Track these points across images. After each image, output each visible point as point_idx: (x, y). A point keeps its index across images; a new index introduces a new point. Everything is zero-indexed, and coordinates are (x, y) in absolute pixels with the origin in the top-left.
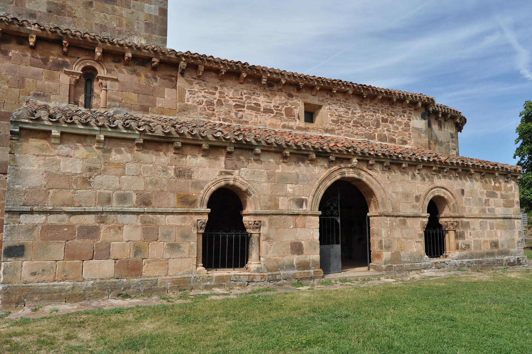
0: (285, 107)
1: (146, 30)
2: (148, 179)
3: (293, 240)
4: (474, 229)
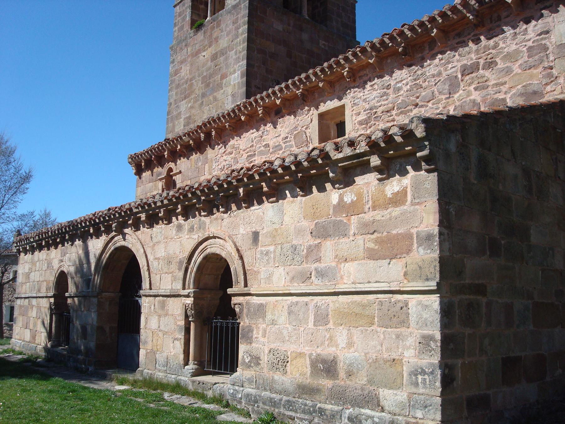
4: (273, 322)
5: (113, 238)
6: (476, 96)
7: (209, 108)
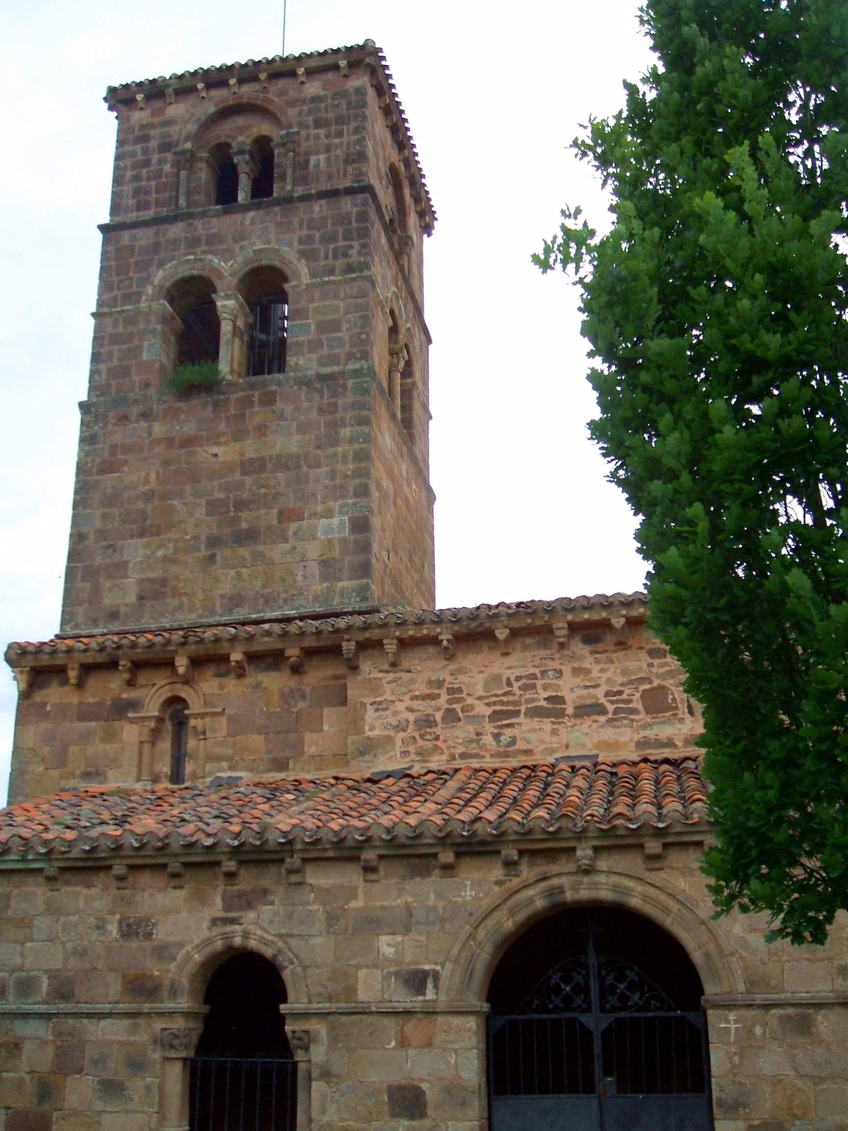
0: (642, 687)
1: (324, 578)
2: (69, 945)
3: (396, 1079)
7: (239, 574)
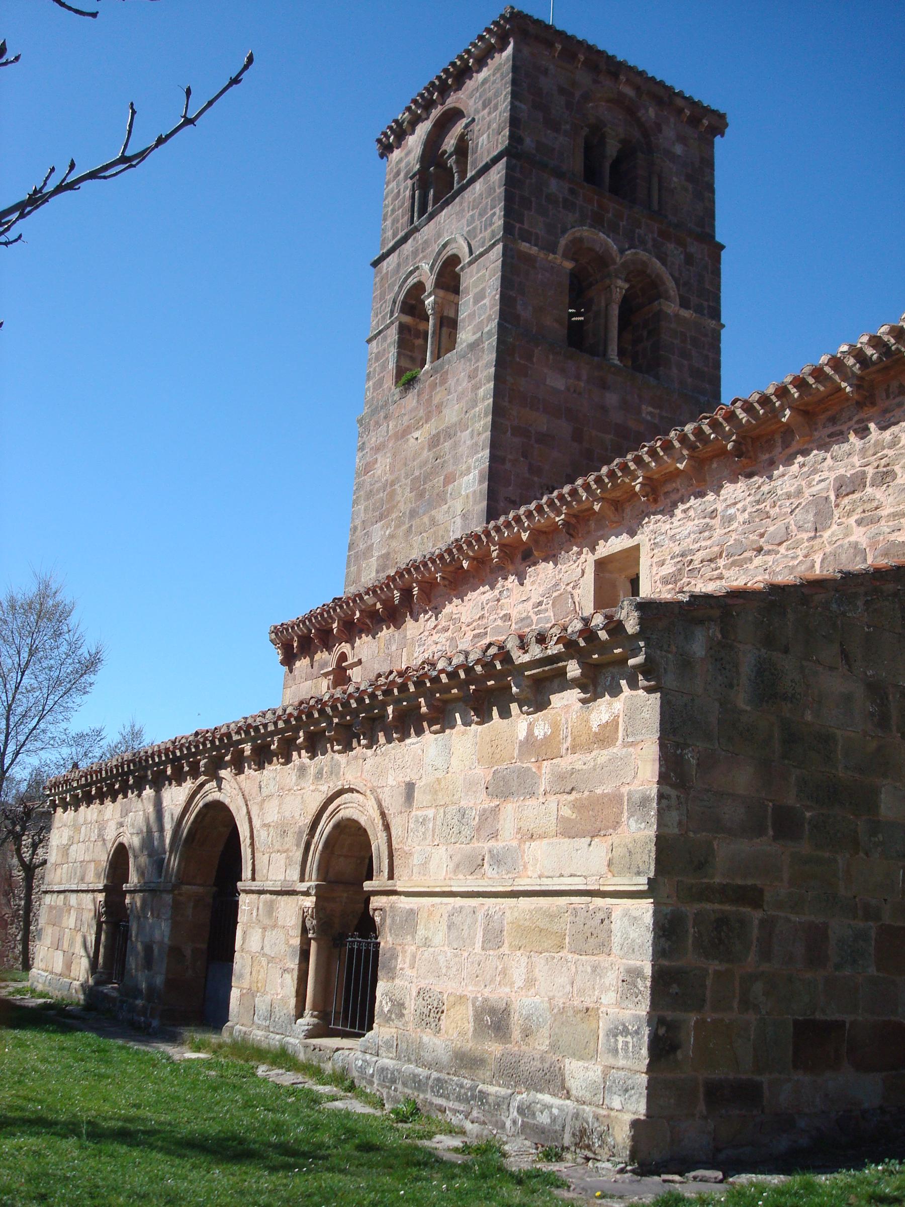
4: (427, 943)
5: (202, 785)
6: (860, 536)
